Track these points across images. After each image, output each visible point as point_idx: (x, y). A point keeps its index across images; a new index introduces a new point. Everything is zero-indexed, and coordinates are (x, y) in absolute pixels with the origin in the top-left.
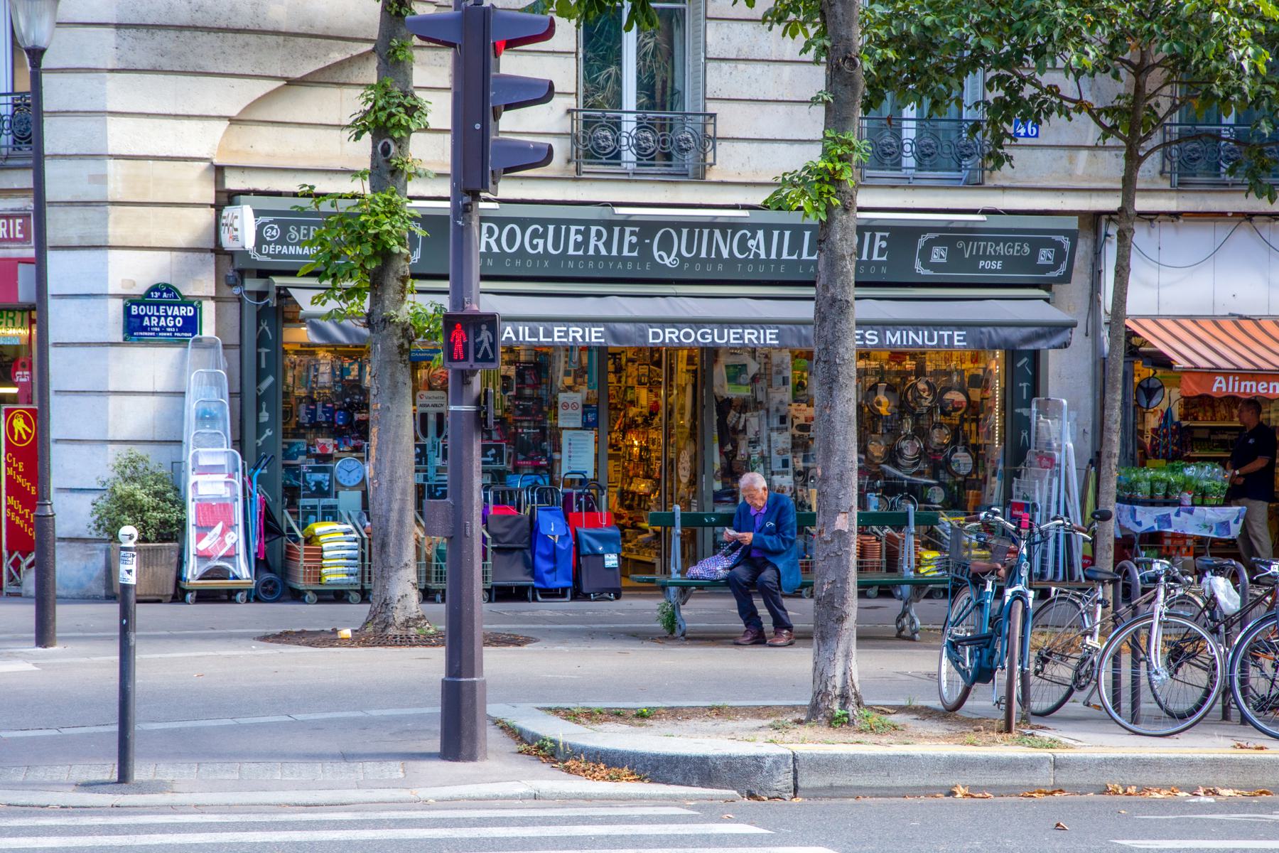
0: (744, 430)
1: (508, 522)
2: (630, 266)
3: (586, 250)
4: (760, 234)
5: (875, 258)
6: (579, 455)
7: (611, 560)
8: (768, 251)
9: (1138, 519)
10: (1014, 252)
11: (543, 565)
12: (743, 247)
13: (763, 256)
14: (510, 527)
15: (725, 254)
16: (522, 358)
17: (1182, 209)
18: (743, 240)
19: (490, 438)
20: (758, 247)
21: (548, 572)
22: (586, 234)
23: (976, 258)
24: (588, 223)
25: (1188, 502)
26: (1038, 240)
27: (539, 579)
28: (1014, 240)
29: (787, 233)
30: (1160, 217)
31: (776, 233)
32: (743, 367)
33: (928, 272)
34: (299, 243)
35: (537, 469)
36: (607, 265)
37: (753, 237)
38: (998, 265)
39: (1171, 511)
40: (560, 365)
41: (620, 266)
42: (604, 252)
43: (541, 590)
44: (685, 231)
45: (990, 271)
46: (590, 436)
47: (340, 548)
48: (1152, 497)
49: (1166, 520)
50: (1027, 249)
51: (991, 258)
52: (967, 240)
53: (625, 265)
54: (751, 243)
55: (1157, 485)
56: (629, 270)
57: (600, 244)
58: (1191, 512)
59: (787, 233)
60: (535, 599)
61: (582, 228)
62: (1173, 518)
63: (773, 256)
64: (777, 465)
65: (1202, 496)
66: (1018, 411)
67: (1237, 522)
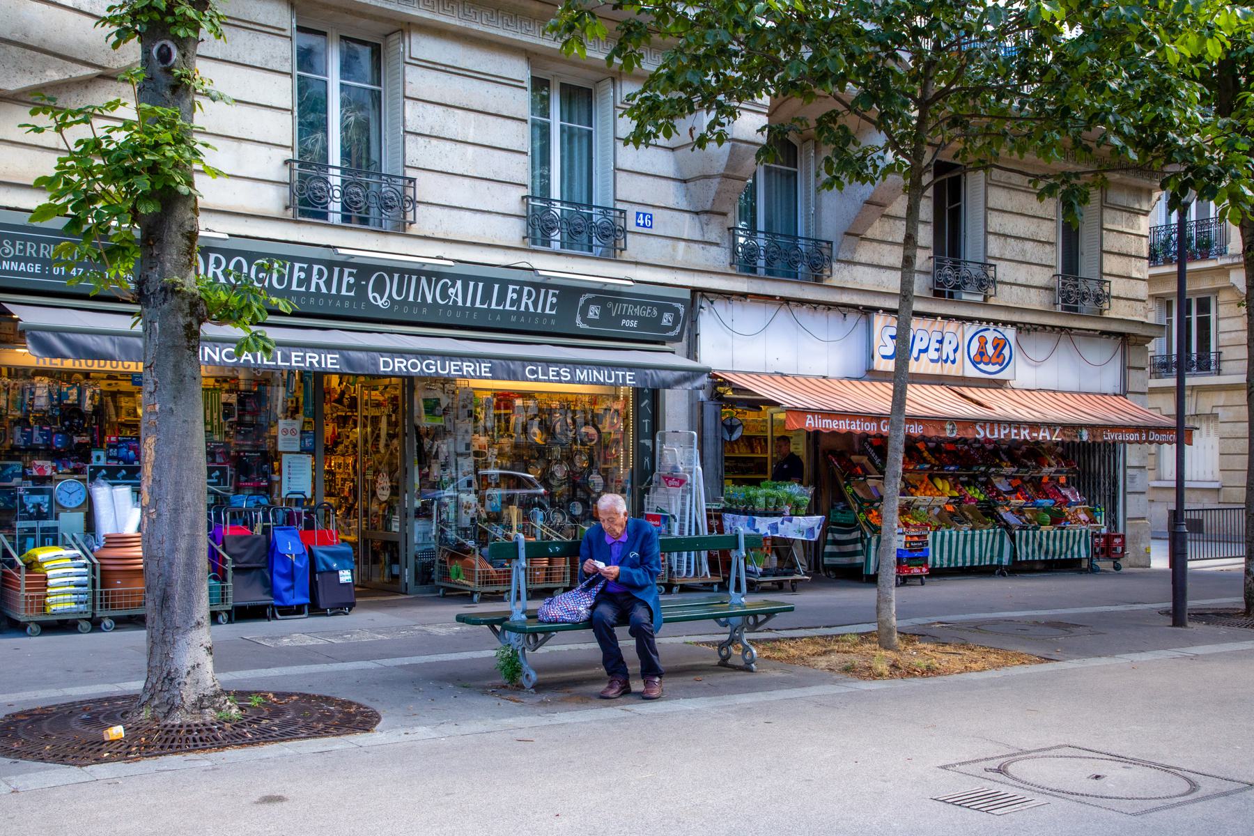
0: (436, 456)
1: (245, 542)
2: (347, 304)
3: (308, 287)
4: (459, 283)
5: (547, 311)
6: (298, 477)
7: (345, 576)
8: (464, 301)
11: (282, 584)
12: (444, 295)
13: (460, 304)
14: (247, 547)
15: (429, 300)
16: (242, 387)
17: (750, 291)
18: (445, 288)
19: (214, 461)
20: (456, 295)
21: (287, 590)
22: (309, 272)
23: (621, 317)
24: (311, 261)
26: (664, 304)
27: (278, 597)
28: (647, 304)
29: (481, 285)
31: (472, 284)
33: (585, 326)
34: (15, 259)
35: (257, 490)
36: (326, 302)
37: (453, 286)
38: (634, 324)
39: (778, 520)
40: (279, 396)
41: (338, 304)
42: (324, 290)
43: (278, 607)
44: (396, 276)
46: (308, 460)
47: (68, 575)
49: (774, 527)
50: (655, 312)
52: (615, 301)
54: (451, 291)
57: (321, 283)
58: (790, 521)
59: (481, 285)
60: (274, 617)
63: (468, 304)
64: (463, 486)
65: (797, 510)
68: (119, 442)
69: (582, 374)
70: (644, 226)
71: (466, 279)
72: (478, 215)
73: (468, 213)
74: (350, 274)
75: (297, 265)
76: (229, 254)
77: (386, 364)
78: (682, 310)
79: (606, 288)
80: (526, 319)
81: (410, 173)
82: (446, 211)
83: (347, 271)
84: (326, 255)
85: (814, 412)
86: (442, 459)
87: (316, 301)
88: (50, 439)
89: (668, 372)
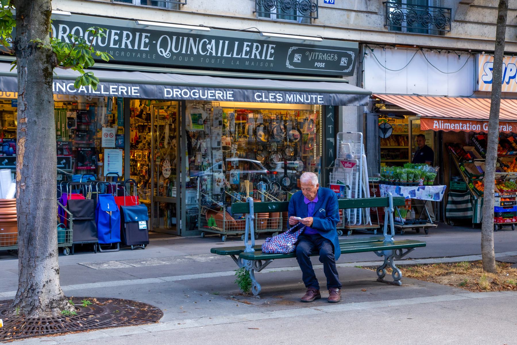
4: (213, 42)
10: (330, 59)
12: (204, 49)
13: (214, 54)
15: (195, 52)
17: (397, 42)
18: (205, 44)
20: (212, 49)
22: (120, 36)
23: (314, 61)
24: (122, 29)
28: (331, 52)
29: (227, 42)
31: (221, 42)
36: (131, 55)
39: (415, 188)
41: (139, 55)
42: (130, 47)
44: (174, 38)
45: (320, 68)
50: (336, 57)
51: (320, 61)
52: (311, 51)
56: (144, 58)
58: (424, 189)
59: (227, 42)
61: (118, 32)
65: (428, 181)
66: (328, 139)
68: (4, 142)
71: (217, 39)
74: (146, 37)
75: (113, 32)
76: (72, 25)
77: (168, 93)
78: (353, 56)
79: (305, 43)
80: (255, 63)
83: (144, 35)
84: (132, 25)
85: (438, 119)
86: (203, 151)
87: (125, 54)
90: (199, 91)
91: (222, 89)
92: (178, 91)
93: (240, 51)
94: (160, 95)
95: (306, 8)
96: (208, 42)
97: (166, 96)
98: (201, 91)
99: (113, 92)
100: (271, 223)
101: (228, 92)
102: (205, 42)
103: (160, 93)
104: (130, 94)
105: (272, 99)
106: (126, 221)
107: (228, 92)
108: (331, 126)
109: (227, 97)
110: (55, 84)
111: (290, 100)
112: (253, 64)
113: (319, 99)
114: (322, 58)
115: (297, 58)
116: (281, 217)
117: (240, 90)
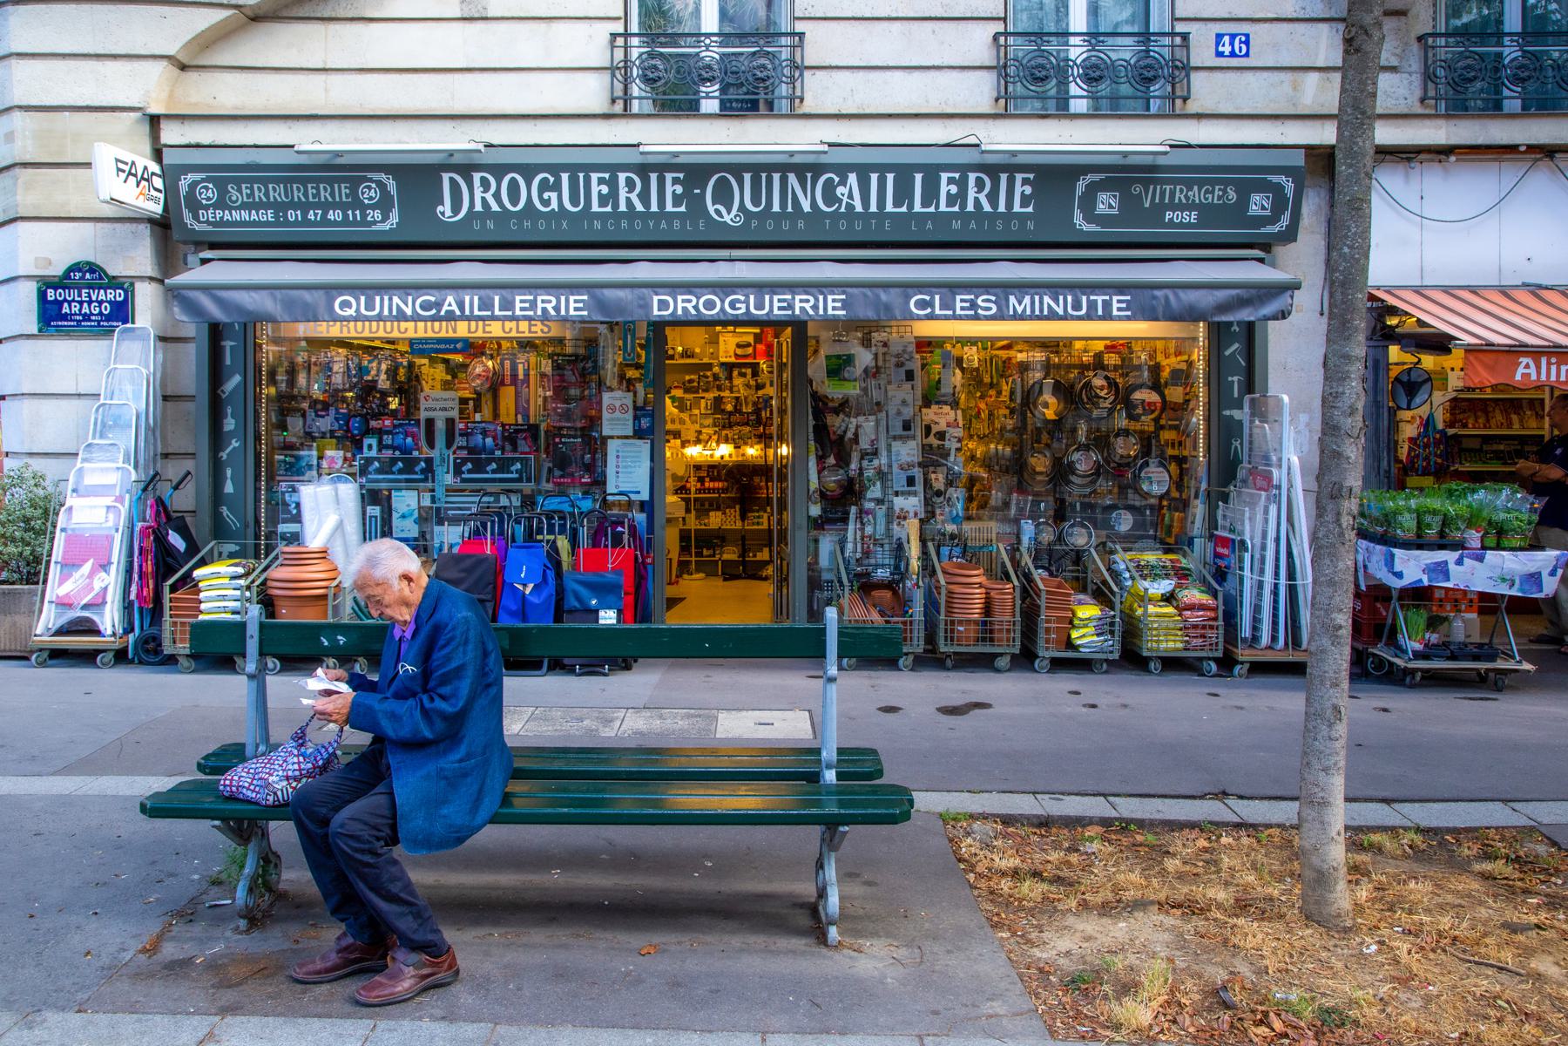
2: (677, 224)
4: (852, 178)
9: (1397, 568)
10: (1214, 198)
12: (830, 197)
13: (859, 208)
15: (806, 207)
17: (1454, 141)
18: (829, 188)
20: (851, 196)
22: (613, 184)
23: (1159, 209)
24: (614, 169)
25: (1476, 544)
28: (1213, 182)
29: (890, 177)
30: (1422, 156)
31: (874, 177)
32: (849, 360)
33: (1093, 228)
34: (244, 206)
36: (645, 225)
37: (843, 182)
39: (1450, 556)
41: (663, 225)
42: (639, 207)
44: (747, 177)
45: (1181, 225)
48: (1419, 536)
49: (1441, 570)
50: (1232, 195)
51: (1182, 207)
52: (1146, 183)
53: (670, 224)
54: (840, 190)
55: (1428, 518)
56: (677, 231)
57: (634, 197)
58: (1480, 559)
59: (890, 177)
61: (607, 176)
62: (1452, 567)
65: (1498, 536)
67: (1553, 573)
68: (395, 427)
69: (383, 304)
70: (1233, 54)
71: (863, 171)
72: (917, 74)
73: (898, 74)
74: (675, 181)
75: (594, 177)
76: (499, 170)
77: (663, 305)
78: (1289, 188)
79: (1132, 160)
80: (980, 224)
81: (800, 27)
82: (861, 73)
83: (669, 177)
84: (632, 157)
85: (1536, 353)
86: (864, 444)
87: (631, 225)
88: (347, 423)
89: (628, 291)
90: (747, 296)
91: (814, 290)
92: (689, 301)
93: (931, 194)
94: (641, 312)
95: (1150, 75)
96: (837, 179)
97: (656, 312)
98: (752, 298)
99: (522, 309)
100: (991, 631)
101: (830, 298)
102: (546, 179)
103: (641, 307)
104: (563, 312)
105: (962, 309)
106: (566, 607)
107: (830, 298)
108: (1235, 379)
109: (825, 309)
110: (390, 299)
111: (1020, 309)
112: (973, 225)
113: (1115, 305)
114: (1187, 197)
115: (1106, 203)
116: (1018, 618)
117: (868, 291)
